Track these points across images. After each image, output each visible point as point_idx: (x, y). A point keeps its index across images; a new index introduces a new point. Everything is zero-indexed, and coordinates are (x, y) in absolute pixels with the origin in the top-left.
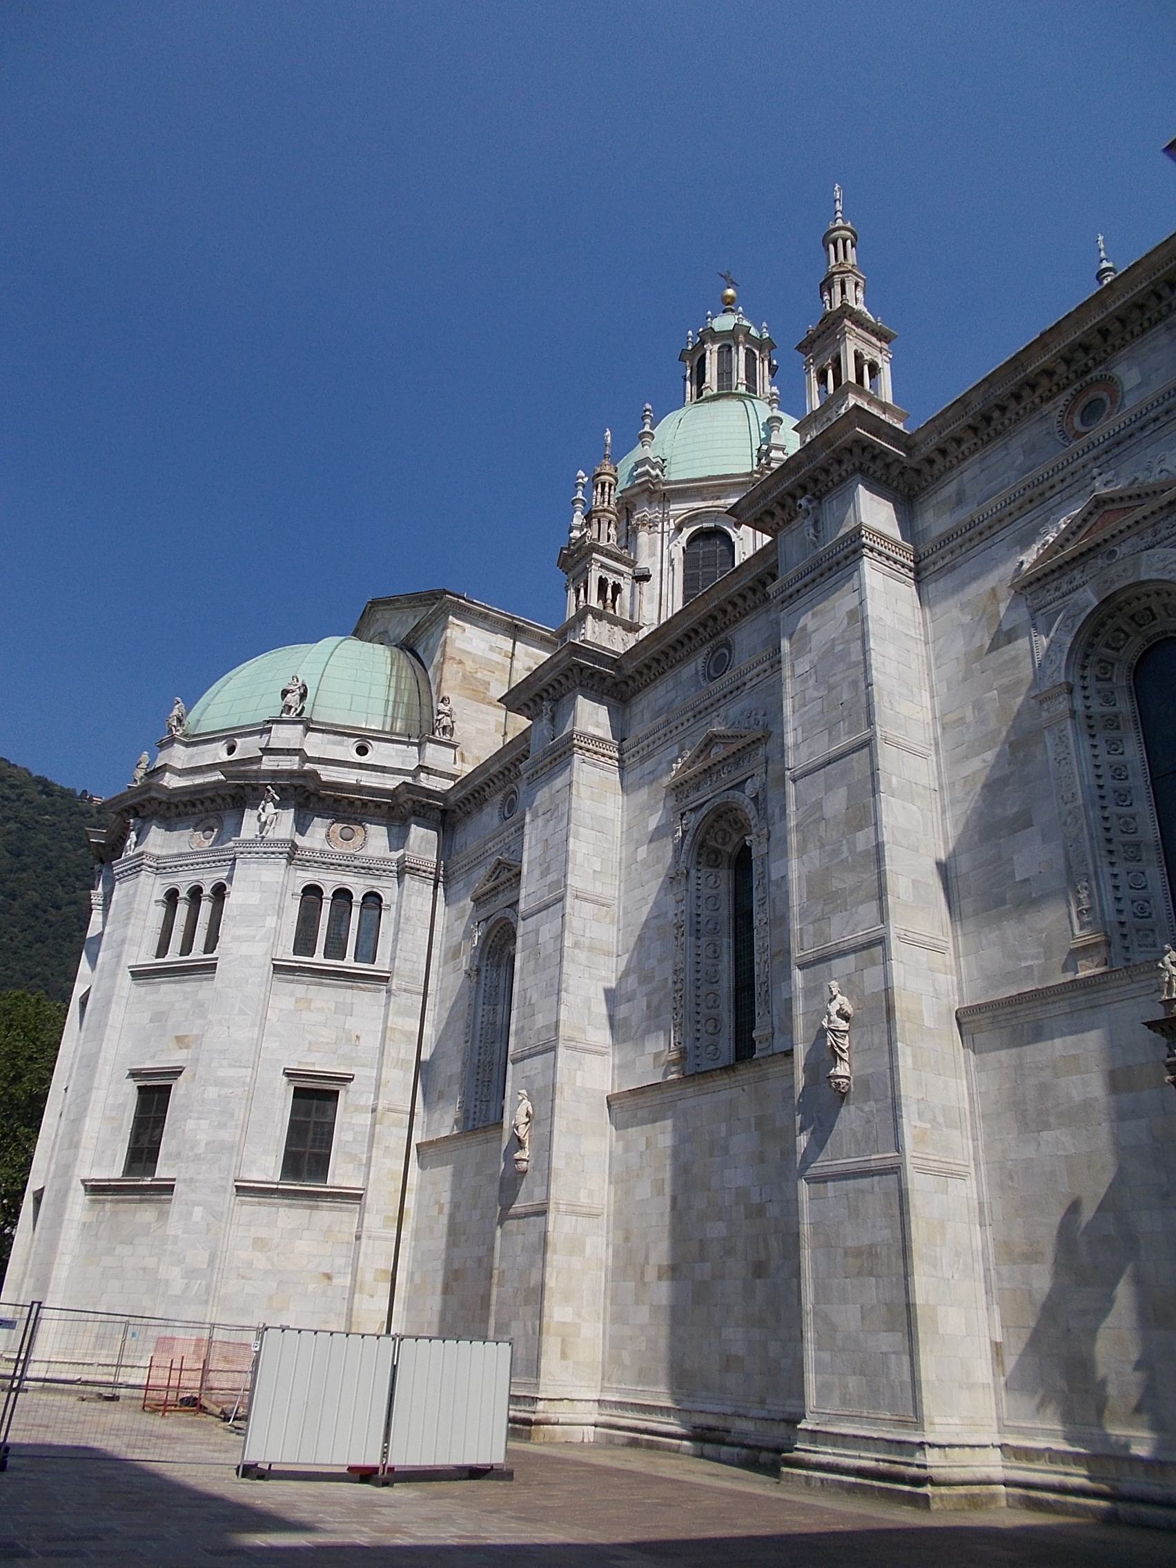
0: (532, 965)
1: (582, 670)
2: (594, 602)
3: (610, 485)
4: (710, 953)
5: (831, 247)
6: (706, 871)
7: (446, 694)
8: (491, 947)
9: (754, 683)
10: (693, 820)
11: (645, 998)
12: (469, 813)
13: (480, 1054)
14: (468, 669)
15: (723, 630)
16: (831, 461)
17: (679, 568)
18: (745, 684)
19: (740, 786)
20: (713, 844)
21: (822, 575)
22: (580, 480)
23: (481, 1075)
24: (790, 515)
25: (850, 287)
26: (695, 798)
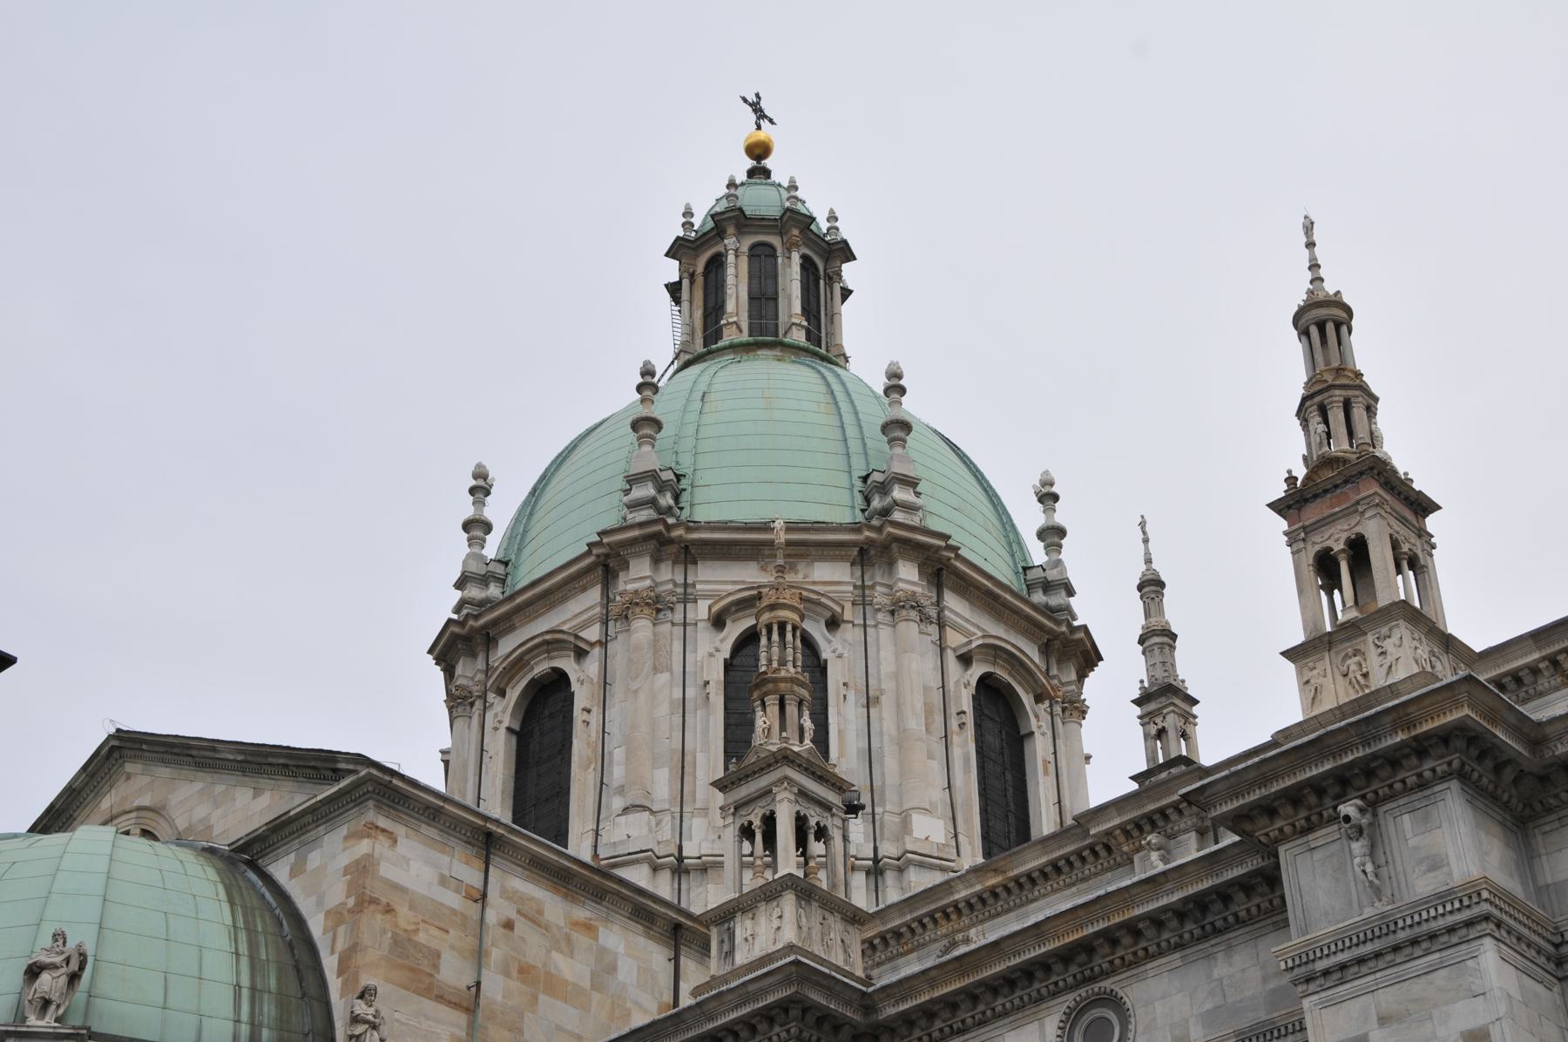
1: (805, 1011)
2: (788, 862)
5: (1314, 331)
7: (366, 980)
14: (403, 923)
15: (1105, 974)
16: (1407, 751)
17: (718, 700)
21: (1396, 949)
24: (1308, 819)
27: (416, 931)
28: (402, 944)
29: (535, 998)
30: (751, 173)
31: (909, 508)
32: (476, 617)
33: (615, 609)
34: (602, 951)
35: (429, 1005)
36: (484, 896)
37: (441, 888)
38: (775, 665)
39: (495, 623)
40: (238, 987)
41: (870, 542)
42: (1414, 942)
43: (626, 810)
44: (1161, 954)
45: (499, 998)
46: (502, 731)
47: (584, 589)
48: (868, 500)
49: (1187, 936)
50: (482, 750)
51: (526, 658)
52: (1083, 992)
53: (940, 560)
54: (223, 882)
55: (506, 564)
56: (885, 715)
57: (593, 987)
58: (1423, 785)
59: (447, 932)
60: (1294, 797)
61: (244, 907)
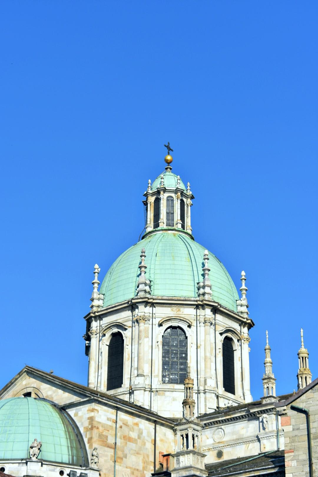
22: (96, 271)
25: (308, 379)
27: (103, 432)
28: (100, 436)
29: (126, 443)
33: (135, 319)
34: (140, 429)
35: (106, 449)
36: (116, 422)
37: (108, 421)
38: (188, 398)
40: (68, 447)
41: (200, 305)
43: (138, 375)
48: (199, 289)
54: (60, 418)
56: (201, 351)
59: (109, 431)
61: (66, 425)
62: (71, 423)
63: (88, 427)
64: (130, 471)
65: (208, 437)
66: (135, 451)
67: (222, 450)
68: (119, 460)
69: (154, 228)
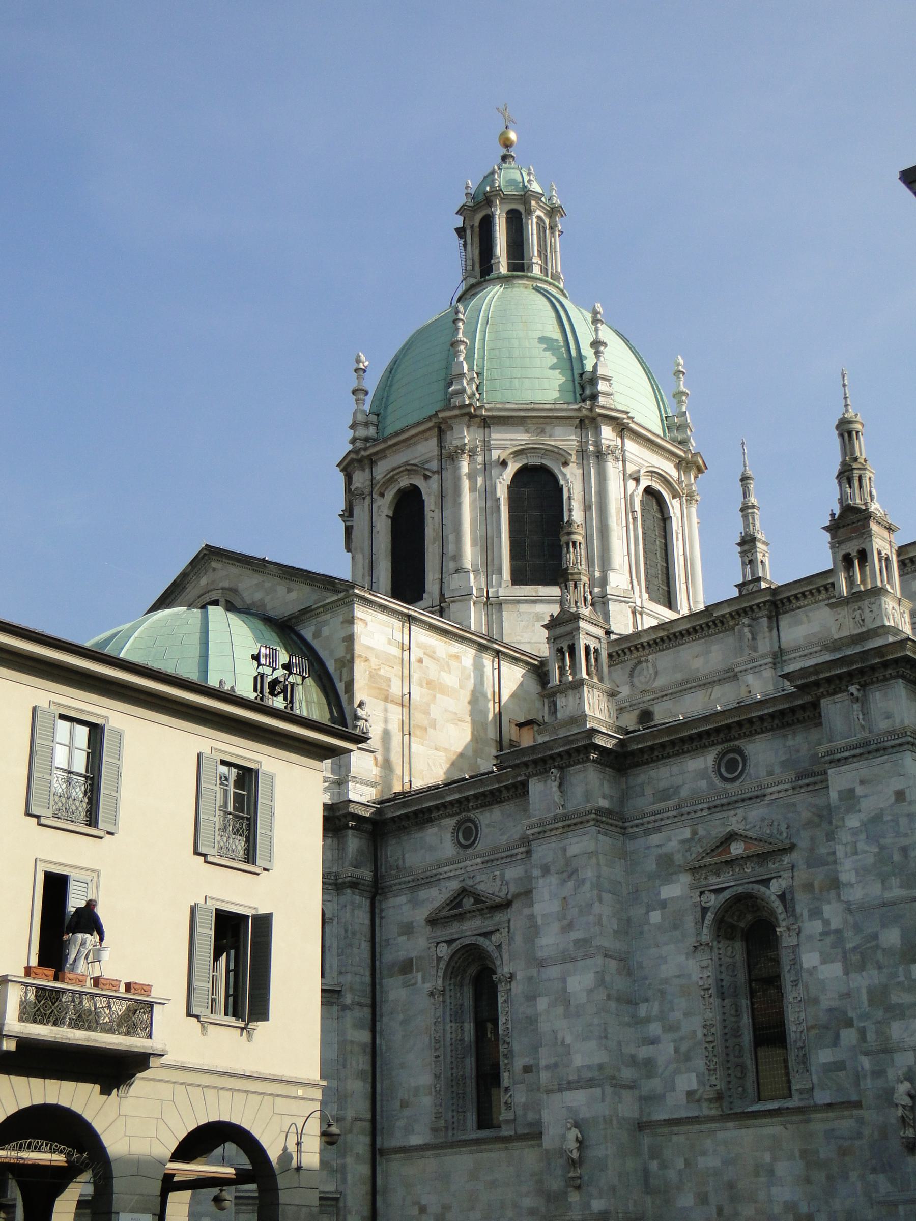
0: (560, 1010)
3: (580, 543)
4: (733, 1012)
5: (846, 435)
6: (723, 944)
8: (454, 967)
9: (774, 797)
10: (713, 901)
11: (672, 1044)
12: (405, 828)
13: (452, 1069)
15: (736, 739)
18: (765, 795)
19: (766, 882)
20: (730, 920)
21: (869, 753)
23: (455, 1088)
26: (715, 881)
27: (379, 669)
28: (373, 676)
29: (435, 696)
30: (504, 158)
31: (608, 395)
32: (365, 449)
39: (376, 453)
41: (587, 417)
42: (877, 750)
44: (762, 732)
45: (418, 699)
46: (384, 517)
47: (427, 439)
48: (583, 388)
49: (775, 726)
50: (372, 526)
51: (396, 477)
52: (725, 745)
53: (623, 424)
54: (281, 641)
55: (378, 415)
57: (461, 687)
58: (886, 679)
60: (829, 680)
62: (306, 651)
63: (344, 657)
64: (444, 758)
65: (618, 682)
66: (456, 714)
67: (651, 708)
68: (418, 732)
69: (481, 278)
